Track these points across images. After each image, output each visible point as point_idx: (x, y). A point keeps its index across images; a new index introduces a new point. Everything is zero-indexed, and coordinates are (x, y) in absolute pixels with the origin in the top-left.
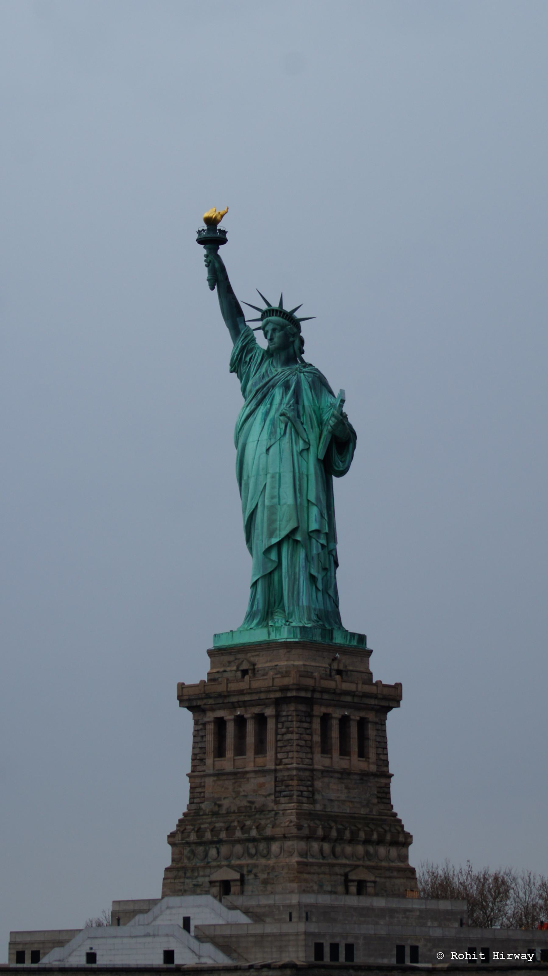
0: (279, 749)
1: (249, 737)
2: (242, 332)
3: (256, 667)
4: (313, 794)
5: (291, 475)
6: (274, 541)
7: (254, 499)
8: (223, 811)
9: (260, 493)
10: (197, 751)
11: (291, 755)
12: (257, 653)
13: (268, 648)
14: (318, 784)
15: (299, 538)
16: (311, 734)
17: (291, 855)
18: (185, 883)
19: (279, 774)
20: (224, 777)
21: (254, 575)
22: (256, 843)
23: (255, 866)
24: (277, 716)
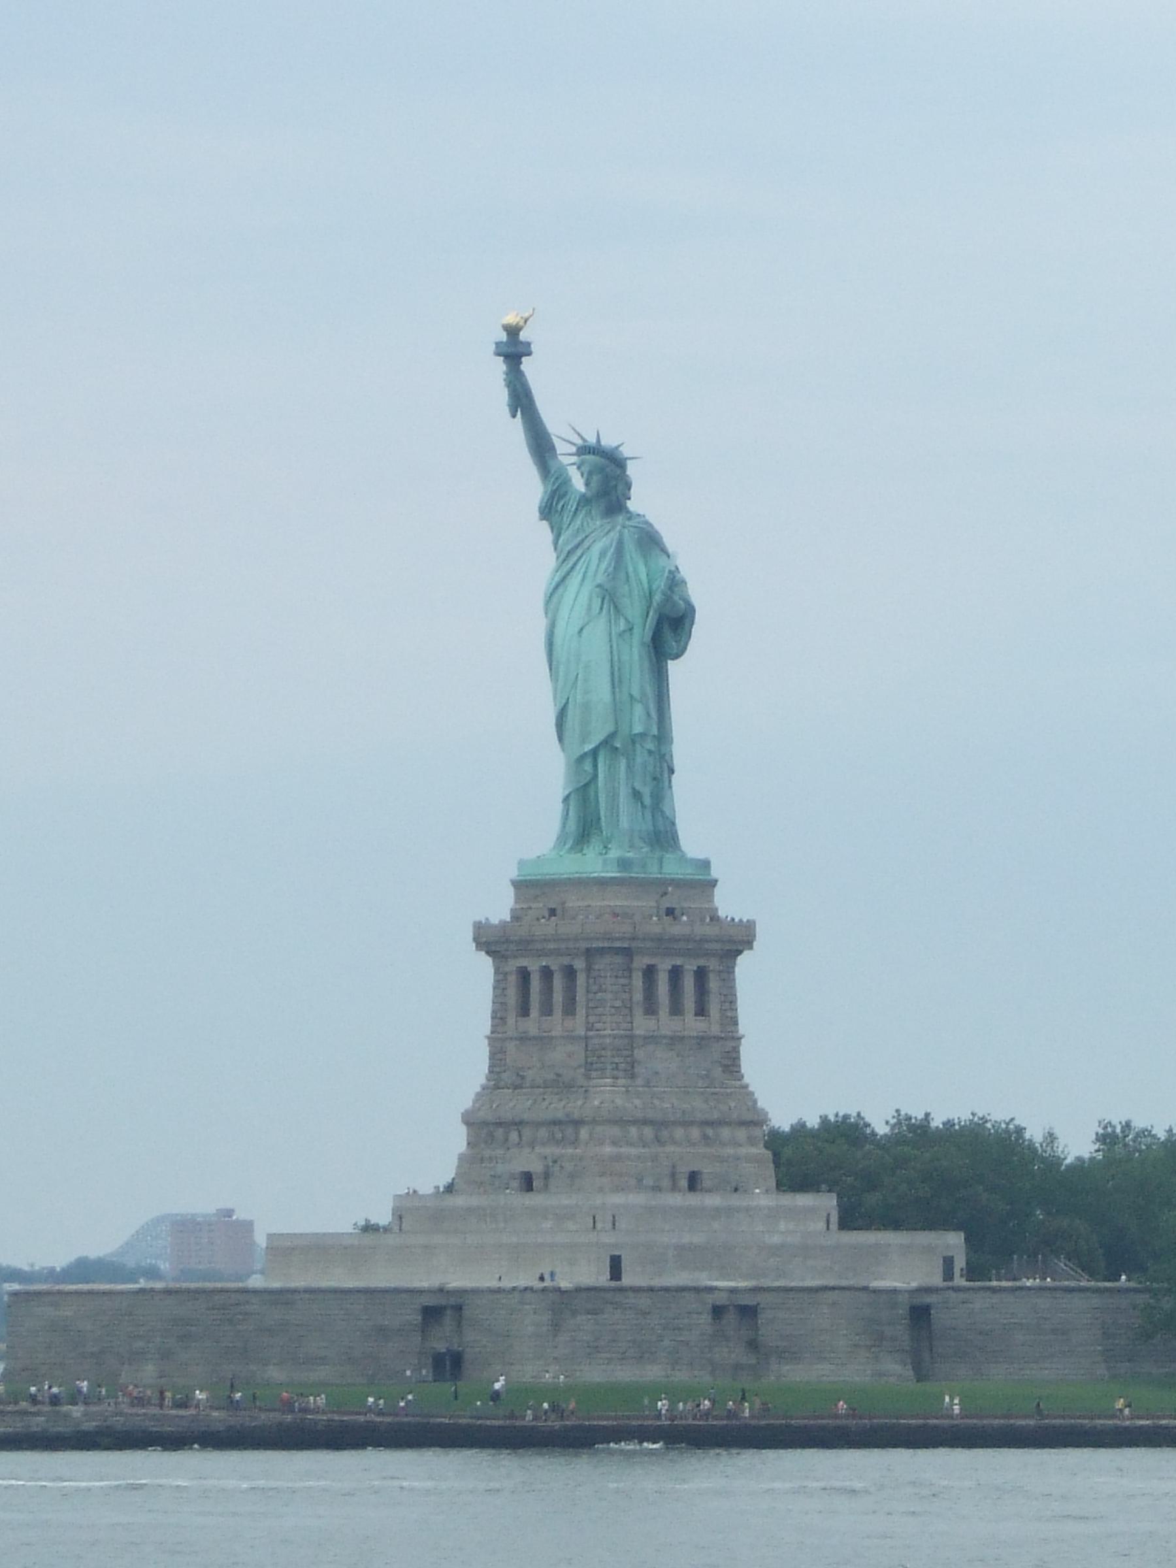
2: (553, 472)
3: (566, 905)
4: (633, 1067)
5: (608, 666)
6: (588, 747)
14: (639, 1054)
15: (618, 745)
16: (630, 991)
24: (589, 969)
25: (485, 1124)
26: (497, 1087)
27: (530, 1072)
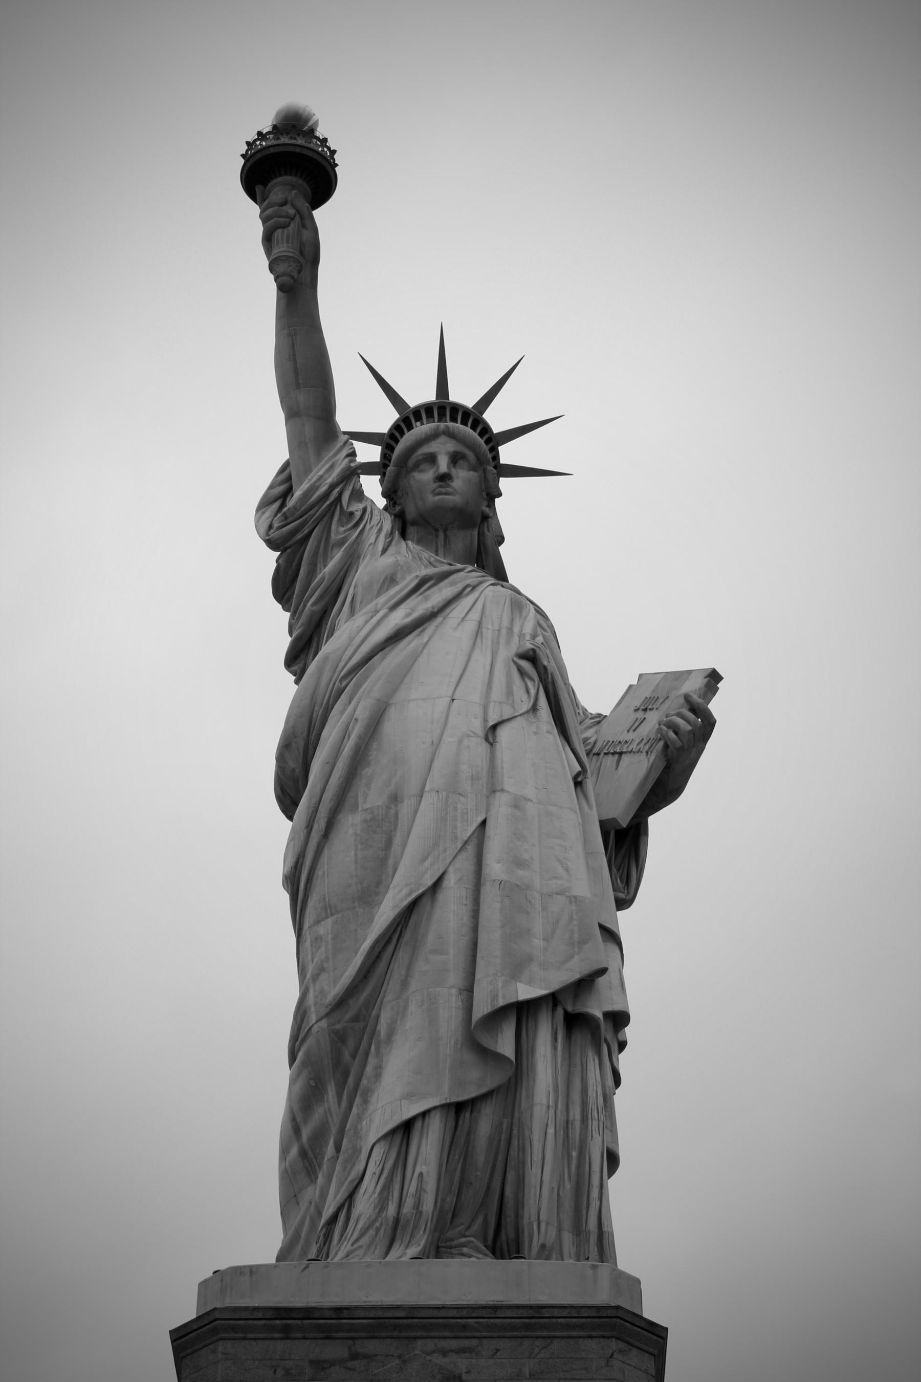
6: (525, 992)
7: (429, 860)
9: (459, 845)
12: (466, 1343)
13: (527, 1327)
21: (409, 1096)
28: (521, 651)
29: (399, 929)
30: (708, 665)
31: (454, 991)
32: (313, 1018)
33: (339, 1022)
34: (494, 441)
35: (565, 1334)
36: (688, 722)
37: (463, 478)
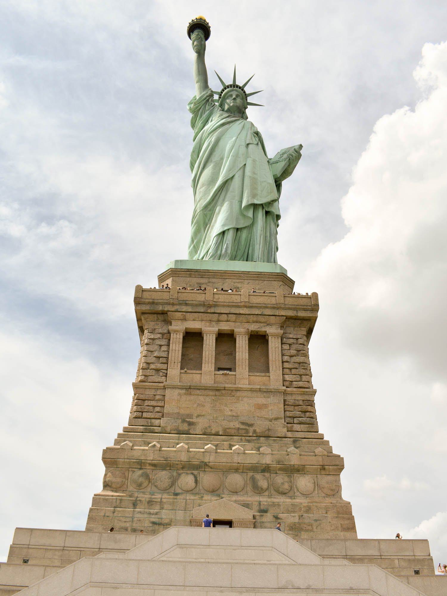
0: (287, 371)
1: (240, 353)
6: (256, 202)
7: (230, 172)
8: (198, 429)
9: (239, 168)
10: (152, 359)
11: (304, 378)
12: (241, 280)
17: (333, 495)
18: (135, 519)
19: (288, 398)
20: (198, 392)
21: (224, 225)
22: (267, 475)
23: (274, 505)
25: (141, 464)
26: (149, 430)
27: (200, 420)
28: (254, 131)
29: (222, 188)
30: (300, 144)
31: (237, 201)
32: (198, 211)
33: (205, 211)
34: (246, 96)
35: (268, 279)
36: (295, 154)
37: (239, 100)
